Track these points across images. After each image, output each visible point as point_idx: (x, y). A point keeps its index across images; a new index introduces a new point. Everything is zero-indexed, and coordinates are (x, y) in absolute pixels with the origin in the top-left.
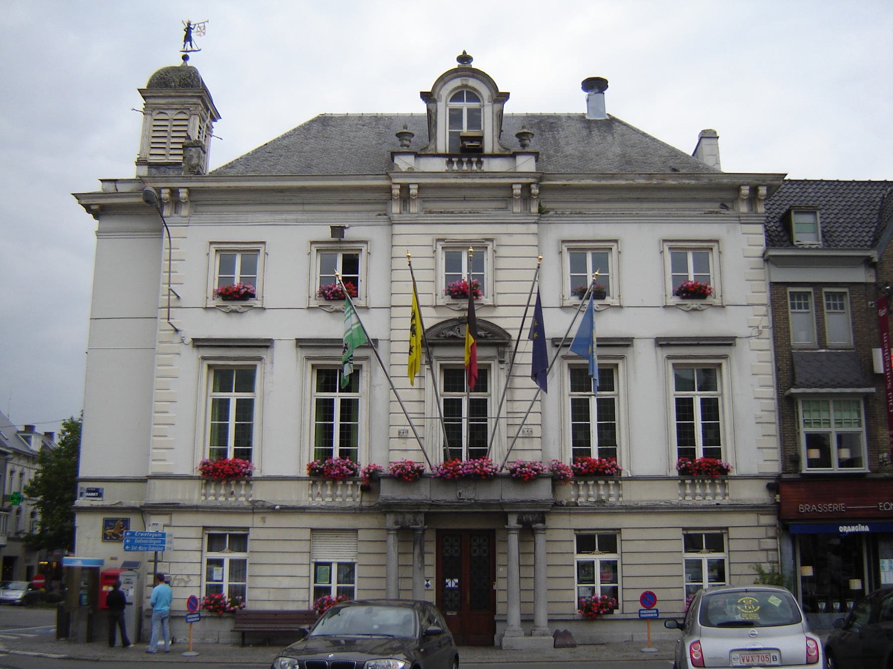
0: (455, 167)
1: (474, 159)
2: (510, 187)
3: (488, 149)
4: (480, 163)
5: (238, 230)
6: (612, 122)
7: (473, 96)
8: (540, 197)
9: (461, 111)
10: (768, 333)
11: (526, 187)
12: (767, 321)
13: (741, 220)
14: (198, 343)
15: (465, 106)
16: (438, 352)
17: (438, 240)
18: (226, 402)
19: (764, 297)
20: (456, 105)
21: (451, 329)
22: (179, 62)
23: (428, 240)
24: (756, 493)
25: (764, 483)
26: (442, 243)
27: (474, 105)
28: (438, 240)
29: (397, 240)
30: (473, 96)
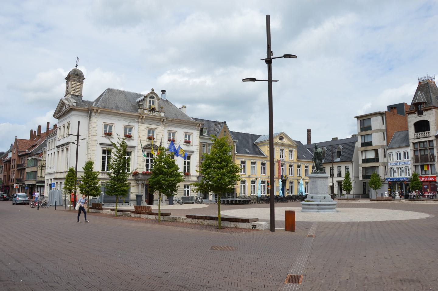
0: (150, 113)
1: (153, 112)
2: (161, 119)
3: (156, 110)
4: (154, 112)
5: (109, 120)
6: (167, 101)
7: (153, 98)
8: (163, 121)
9: (151, 100)
10: (199, 151)
11: (164, 119)
12: (199, 149)
13: (196, 129)
14: (101, 144)
15: (152, 100)
16: (147, 150)
17: (147, 128)
18: (105, 156)
19: (199, 144)
20: (150, 99)
21: (149, 146)
22: (75, 68)
23: (145, 127)
24: (195, 179)
25: (196, 177)
26: (148, 128)
27: (153, 100)
28: (147, 128)
29: (140, 126)
30: (153, 98)
